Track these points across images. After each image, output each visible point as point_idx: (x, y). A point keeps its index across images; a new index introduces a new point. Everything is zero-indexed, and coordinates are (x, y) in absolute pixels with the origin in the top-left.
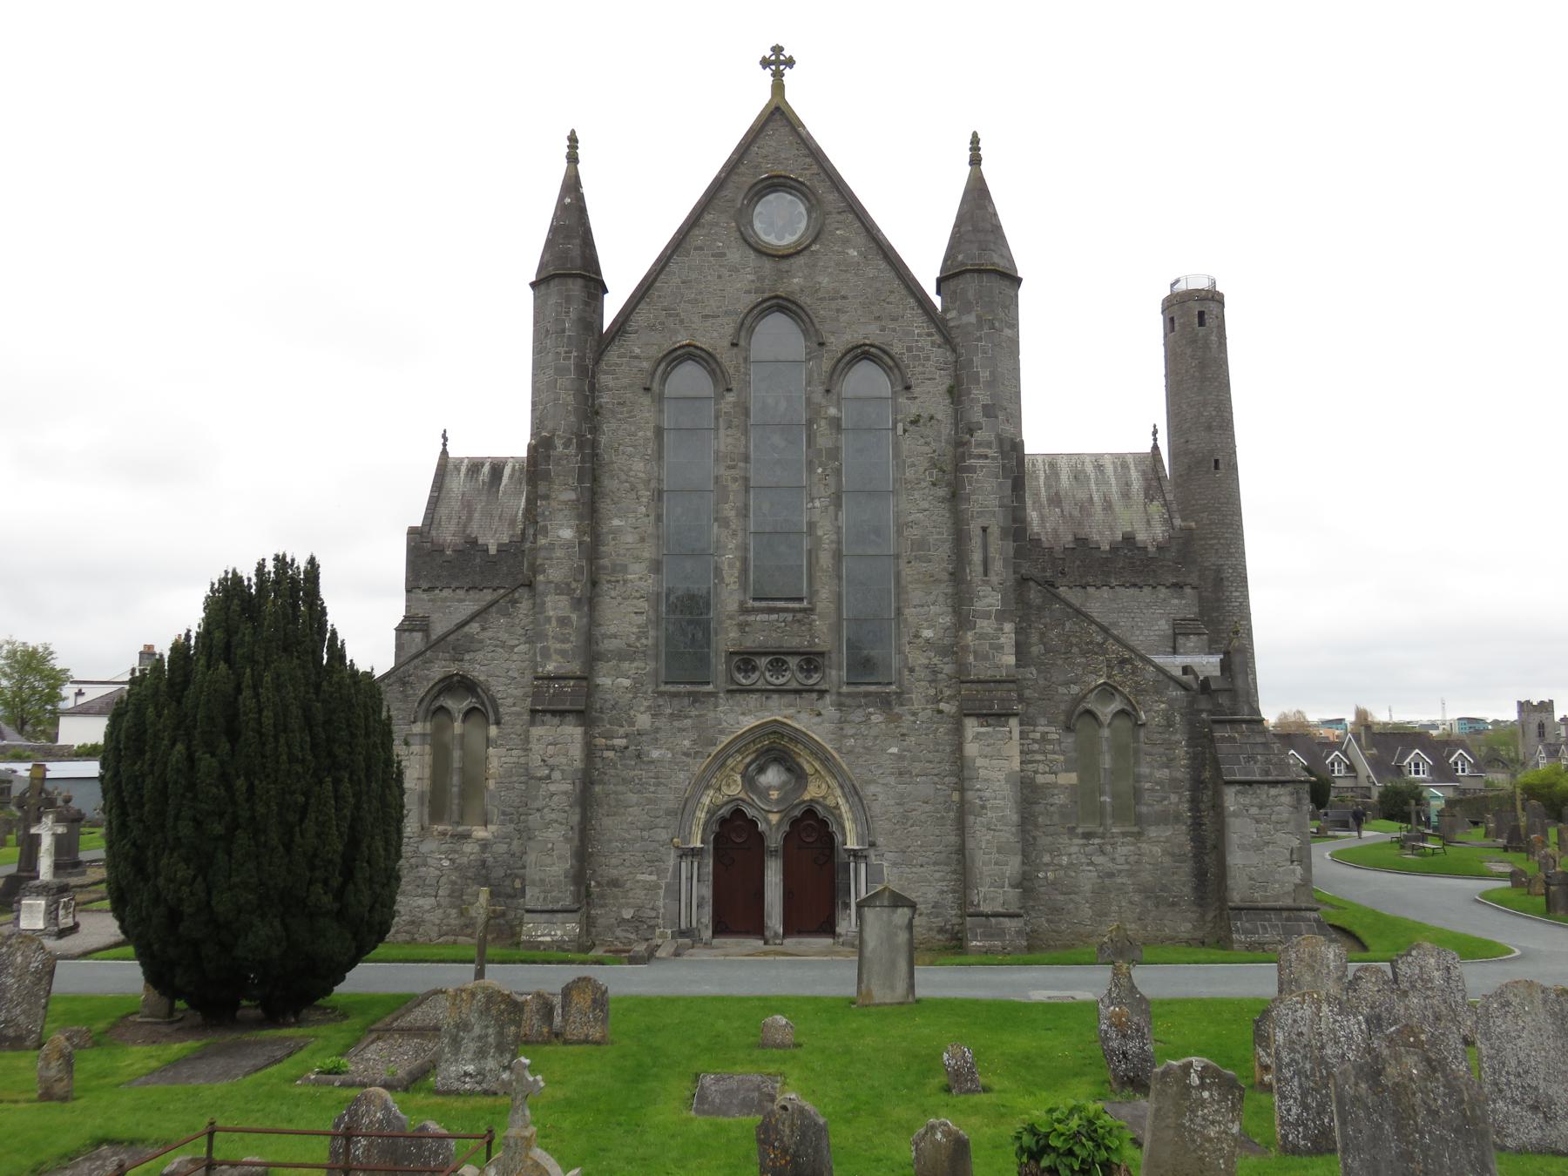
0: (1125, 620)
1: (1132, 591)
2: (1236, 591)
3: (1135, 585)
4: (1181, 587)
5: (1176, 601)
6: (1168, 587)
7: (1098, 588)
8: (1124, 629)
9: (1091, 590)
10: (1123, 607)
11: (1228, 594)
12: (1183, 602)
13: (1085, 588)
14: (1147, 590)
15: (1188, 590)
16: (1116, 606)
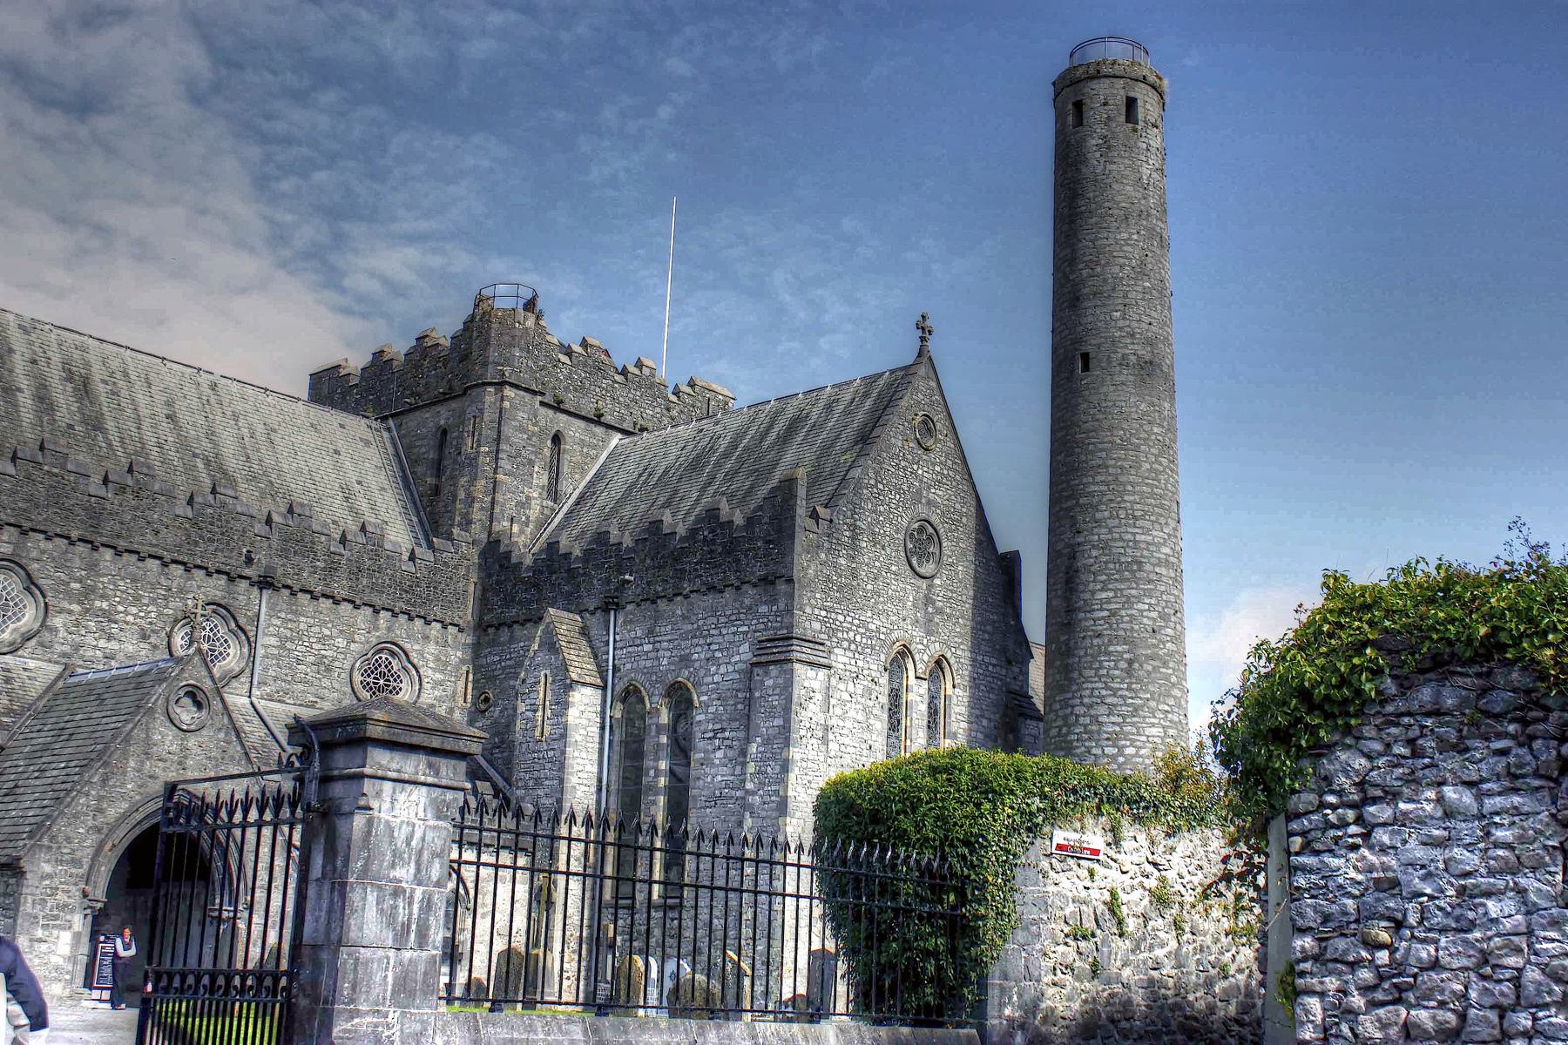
0: (699, 649)
1: (710, 599)
2: (1102, 590)
3: (712, 588)
4: (773, 583)
5: (763, 609)
6: (755, 585)
7: (670, 600)
8: (697, 665)
9: (662, 604)
10: (699, 627)
11: (1087, 596)
12: (775, 608)
13: (654, 602)
14: (729, 594)
15: (782, 587)
16: (690, 627)
